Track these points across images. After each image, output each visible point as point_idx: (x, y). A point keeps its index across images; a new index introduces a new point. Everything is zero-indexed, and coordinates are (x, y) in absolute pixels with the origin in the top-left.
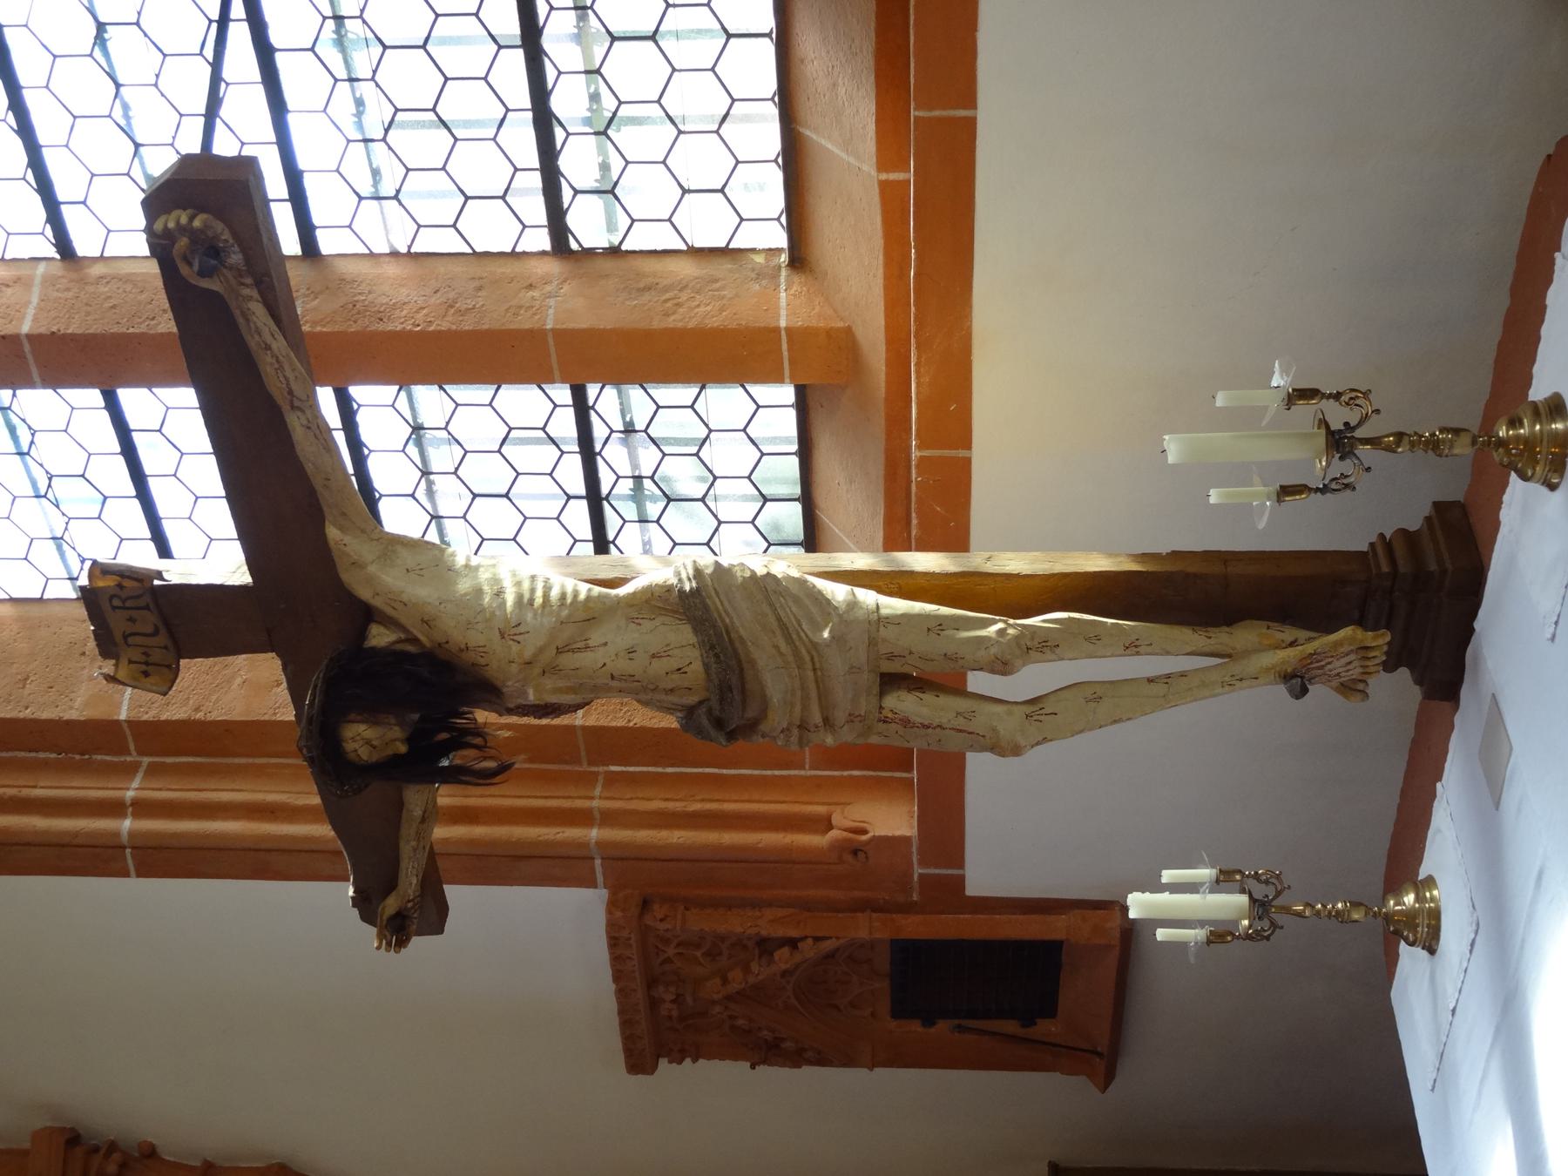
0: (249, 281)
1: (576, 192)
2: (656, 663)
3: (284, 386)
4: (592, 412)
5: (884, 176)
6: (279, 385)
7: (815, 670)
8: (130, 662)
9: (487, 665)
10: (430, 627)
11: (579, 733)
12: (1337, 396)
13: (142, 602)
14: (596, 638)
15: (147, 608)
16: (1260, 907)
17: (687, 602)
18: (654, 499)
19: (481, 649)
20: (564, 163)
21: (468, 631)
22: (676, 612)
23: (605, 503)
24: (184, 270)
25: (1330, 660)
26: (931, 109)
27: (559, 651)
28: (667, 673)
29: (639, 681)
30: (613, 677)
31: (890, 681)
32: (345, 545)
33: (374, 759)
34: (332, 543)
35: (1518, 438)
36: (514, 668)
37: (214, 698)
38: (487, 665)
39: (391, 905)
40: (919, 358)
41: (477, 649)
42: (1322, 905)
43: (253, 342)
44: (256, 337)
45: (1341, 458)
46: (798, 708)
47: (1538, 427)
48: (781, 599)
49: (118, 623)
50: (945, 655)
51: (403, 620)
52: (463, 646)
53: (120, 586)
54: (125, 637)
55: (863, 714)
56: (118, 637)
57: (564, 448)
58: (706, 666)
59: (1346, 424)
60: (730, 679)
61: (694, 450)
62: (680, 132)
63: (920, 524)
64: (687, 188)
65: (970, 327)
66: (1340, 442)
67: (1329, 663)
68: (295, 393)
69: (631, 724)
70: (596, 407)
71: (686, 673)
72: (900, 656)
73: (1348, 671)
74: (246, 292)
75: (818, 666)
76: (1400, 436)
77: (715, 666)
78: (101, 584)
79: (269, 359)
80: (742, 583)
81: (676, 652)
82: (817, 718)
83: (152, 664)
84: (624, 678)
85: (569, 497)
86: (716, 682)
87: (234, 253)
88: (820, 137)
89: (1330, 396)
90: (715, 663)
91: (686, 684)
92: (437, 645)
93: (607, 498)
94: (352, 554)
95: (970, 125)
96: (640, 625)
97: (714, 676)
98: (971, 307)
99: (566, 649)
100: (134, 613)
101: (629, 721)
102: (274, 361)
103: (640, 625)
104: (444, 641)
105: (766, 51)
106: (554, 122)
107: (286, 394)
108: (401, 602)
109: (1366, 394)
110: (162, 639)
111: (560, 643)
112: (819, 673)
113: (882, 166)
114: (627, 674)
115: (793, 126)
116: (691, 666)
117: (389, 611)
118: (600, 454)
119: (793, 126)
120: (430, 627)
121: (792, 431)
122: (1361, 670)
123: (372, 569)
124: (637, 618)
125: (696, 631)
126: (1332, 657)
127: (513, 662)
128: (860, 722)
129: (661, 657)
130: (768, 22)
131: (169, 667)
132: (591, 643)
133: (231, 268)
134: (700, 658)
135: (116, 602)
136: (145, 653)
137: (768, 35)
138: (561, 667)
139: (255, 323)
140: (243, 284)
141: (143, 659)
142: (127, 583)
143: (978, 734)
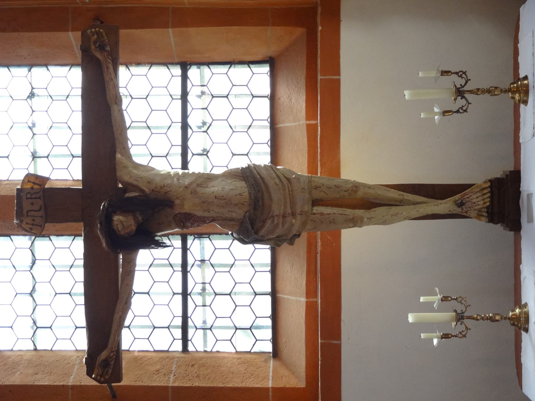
0: (110, 58)
1: (193, 155)
3: (115, 94)
5: (308, 122)
6: (113, 93)
7: (289, 191)
8: (27, 224)
11: (170, 390)
12: (457, 73)
13: (38, 195)
14: (211, 184)
15: (40, 198)
16: (460, 318)
18: (210, 294)
19: (169, 185)
20: (190, 143)
23: (189, 297)
24: (93, 47)
25: (471, 194)
26: (325, 76)
27: (197, 185)
30: (216, 197)
31: (316, 203)
33: (122, 233)
35: (514, 87)
36: (181, 189)
37: (7, 378)
38: (171, 191)
39: (104, 355)
40: (321, 170)
42: (484, 315)
43: (107, 78)
44: (110, 76)
45: (461, 99)
46: (282, 208)
47: (519, 83)
48: (278, 171)
49: (26, 205)
50: (335, 185)
51: (140, 185)
52: (162, 186)
53: (32, 188)
54: (27, 212)
55: (306, 211)
56: (25, 212)
57: (175, 269)
58: (250, 194)
59: (461, 85)
60: (258, 196)
61: (228, 269)
62: (234, 132)
63: (322, 245)
64: (234, 153)
65: (340, 158)
66: (460, 92)
67: (471, 196)
68: (117, 98)
69: (194, 385)
70: (190, 249)
71: (242, 195)
72: (319, 187)
73: (478, 202)
74: (109, 61)
75: (290, 190)
76: (478, 89)
77: (253, 191)
78: (25, 187)
79: (112, 84)
80: (264, 166)
81: (239, 188)
82: (289, 211)
83: (34, 225)
85: (174, 294)
87: (108, 47)
88: (284, 124)
89: (454, 73)
90: (253, 190)
93: (190, 294)
95: (338, 81)
98: (339, 149)
99: (200, 185)
100: (34, 201)
101: (193, 385)
102: (113, 85)
103: (226, 181)
104: (155, 187)
105: (266, 103)
106: (189, 128)
107: (115, 97)
108: (140, 177)
109: (465, 73)
110: (42, 213)
111: (198, 182)
112: (291, 193)
113: (307, 119)
115: (274, 127)
117: (135, 183)
118: (189, 272)
119: (274, 127)
120: (150, 184)
121: (269, 261)
122: (482, 202)
123: (130, 169)
125: (246, 183)
126: (471, 193)
127: (181, 187)
128: (305, 214)
130: (267, 91)
131: (41, 226)
132: (209, 186)
133: (107, 51)
134: (248, 191)
135: (29, 196)
136: (33, 220)
137: (267, 97)
139: (110, 71)
140: (109, 58)
141: (31, 222)
142: (36, 187)
143: (348, 215)
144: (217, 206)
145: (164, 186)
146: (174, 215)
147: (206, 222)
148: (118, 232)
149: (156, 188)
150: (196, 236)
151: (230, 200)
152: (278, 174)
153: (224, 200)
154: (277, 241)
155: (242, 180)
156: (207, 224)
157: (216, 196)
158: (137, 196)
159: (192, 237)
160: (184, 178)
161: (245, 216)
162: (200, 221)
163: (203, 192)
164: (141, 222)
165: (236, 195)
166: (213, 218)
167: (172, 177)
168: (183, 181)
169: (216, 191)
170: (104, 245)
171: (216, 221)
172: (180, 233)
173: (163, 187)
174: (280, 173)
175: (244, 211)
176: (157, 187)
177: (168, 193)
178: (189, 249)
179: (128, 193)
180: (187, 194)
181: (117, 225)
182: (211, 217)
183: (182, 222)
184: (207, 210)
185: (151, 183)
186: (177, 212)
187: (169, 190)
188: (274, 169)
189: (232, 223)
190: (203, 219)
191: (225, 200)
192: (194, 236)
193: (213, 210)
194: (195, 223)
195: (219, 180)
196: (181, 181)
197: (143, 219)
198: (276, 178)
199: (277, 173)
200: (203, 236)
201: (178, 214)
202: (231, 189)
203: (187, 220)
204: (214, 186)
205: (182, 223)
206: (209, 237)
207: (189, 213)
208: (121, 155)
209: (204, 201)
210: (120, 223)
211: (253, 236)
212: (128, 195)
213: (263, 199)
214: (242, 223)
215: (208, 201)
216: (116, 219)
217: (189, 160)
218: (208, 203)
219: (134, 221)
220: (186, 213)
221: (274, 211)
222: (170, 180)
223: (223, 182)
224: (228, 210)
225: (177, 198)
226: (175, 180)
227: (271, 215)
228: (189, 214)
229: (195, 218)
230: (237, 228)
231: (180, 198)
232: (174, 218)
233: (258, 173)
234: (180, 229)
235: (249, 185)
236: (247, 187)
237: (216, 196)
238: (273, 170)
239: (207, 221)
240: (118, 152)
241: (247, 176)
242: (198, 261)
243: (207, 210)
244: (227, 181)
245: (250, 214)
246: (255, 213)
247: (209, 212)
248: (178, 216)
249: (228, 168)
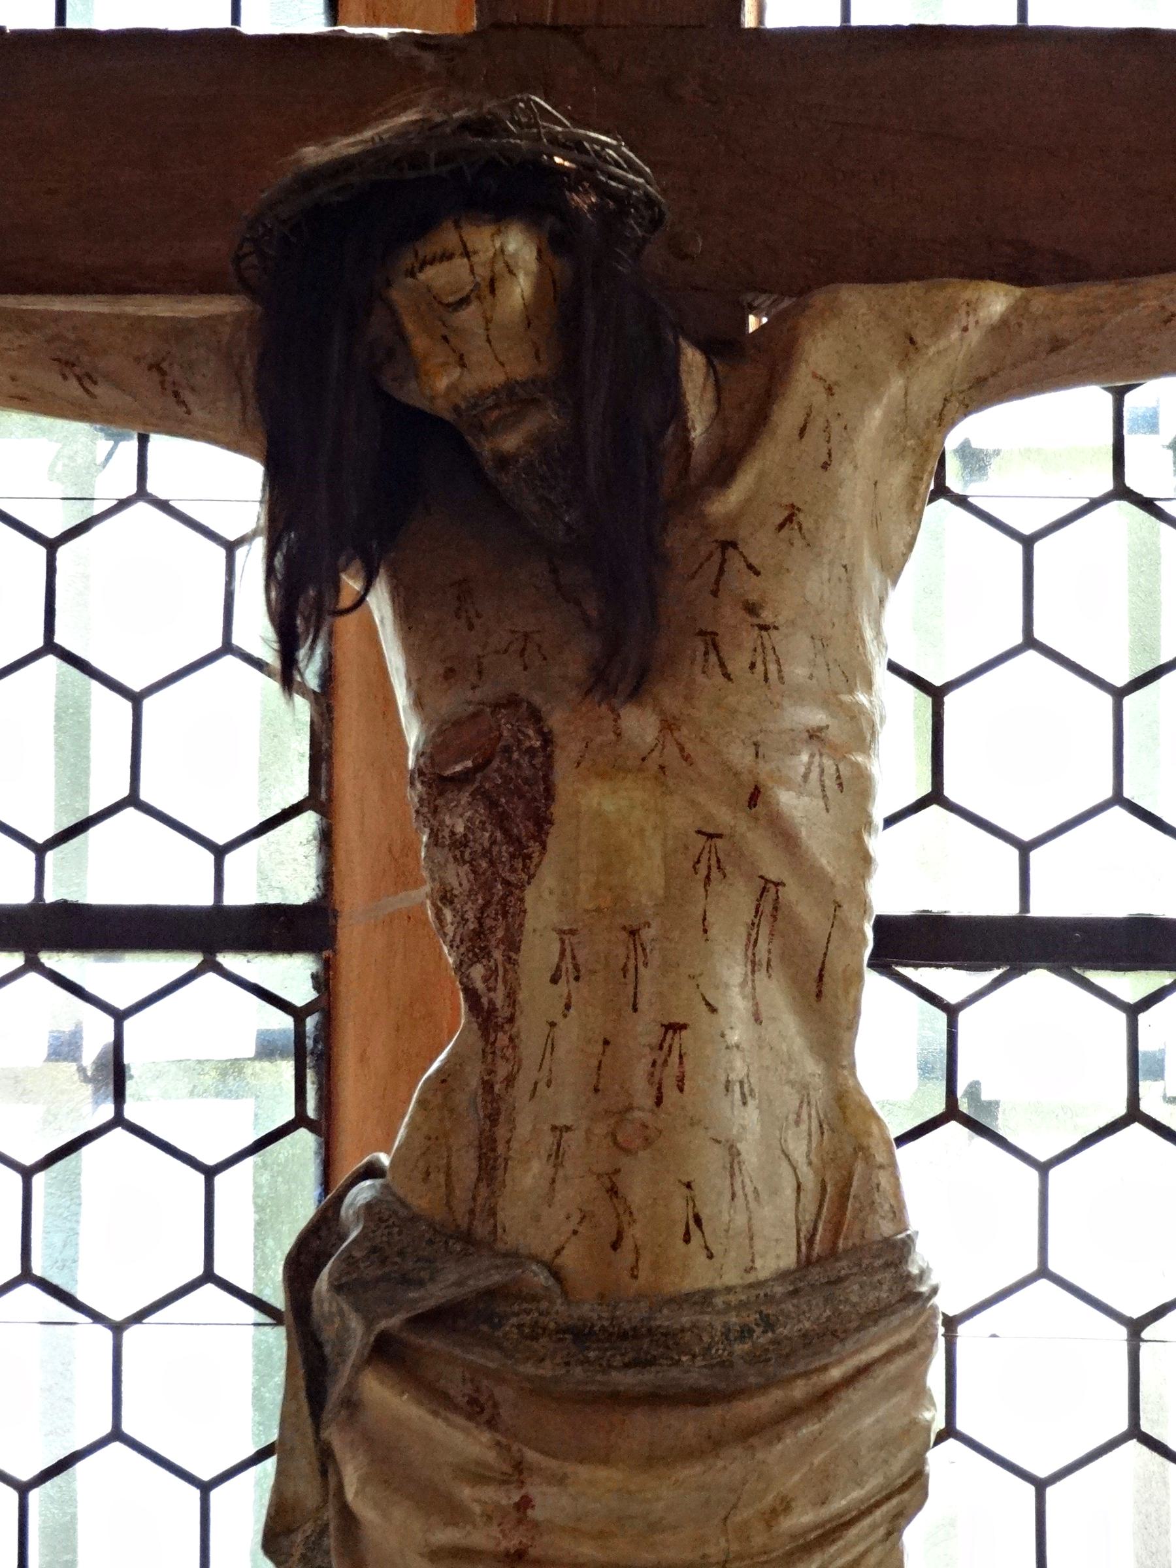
2: (715, 1157)
4: (192, 961)
9: (727, 676)
10: (781, 526)
17: (878, 1263)
19: (772, 667)
21: (808, 641)
22: (836, 1228)
27: (768, 887)
28: (688, 1186)
29: (659, 1101)
30: (676, 1028)
32: (965, 329)
34: (970, 291)
36: (740, 755)
38: (727, 676)
41: (771, 657)
48: (882, 1531)
52: (767, 616)
58: (705, 1298)
60: (678, 1363)
70: (211, 977)
71: (687, 1239)
77: (719, 1327)
80: (914, 1422)
81: (741, 1220)
84: (674, 1058)
86: (664, 1319)
91: (635, 1233)
92: (721, 535)
94: (942, 344)
96: (797, 1123)
97: (686, 1320)
99: (767, 908)
103: (797, 1123)
108: (830, 455)
111: (791, 893)
114: (688, 1067)
116: (702, 1257)
117: (787, 416)
118: (33, 964)
120: (781, 526)
123: (896, 385)
124: (810, 1116)
125: (783, 1276)
129: (732, 1176)
132: (761, 975)
134: (718, 1284)
138: (716, 886)
144: (606, 1042)
145: (764, 628)
146: (537, 699)
147: (477, 959)
148: (408, 260)
149: (750, 567)
150: (311, 1023)
151: (648, 1142)
152: (853, 1532)
153: (654, 1092)
154: (309, 1528)
155: (811, 1241)
156: (459, 966)
157: (684, 1027)
158: (686, 430)
159: (302, 993)
160: (830, 783)
161: (515, 1257)
162: (483, 909)
163: (713, 932)
164: (485, 448)
165: (688, 1186)
166: (507, 1013)
167: (836, 693)
168: (802, 770)
169: (723, 1036)
170: (312, 154)
171: (480, 1044)
172: (337, 896)
173: (756, 621)
174: (860, 1548)
175: (558, 1252)
176: (757, 573)
177: (713, 658)
178: (210, 965)
179: (710, 364)
180: (702, 798)
181: (467, 254)
182: (511, 997)
183: (478, 768)
184: (568, 964)
185: (784, 532)
186: (556, 720)
187: (738, 663)
188: (894, 1502)
189: (466, 1165)
190: (500, 933)
191: (649, 1102)
192: (309, 1009)
193: (568, 1006)
194: (467, 867)
195: (811, 1067)
196: (805, 758)
197: (503, 461)
198: (825, 1512)
199: (866, 1522)
200: (310, 1076)
201: (540, 732)
202: (733, 1153)
203: (492, 804)
204: (757, 1019)
205: (469, 764)
206: (300, 1120)
207: (551, 823)
208: (1004, 322)
209: (647, 934)
210: (482, 272)
211: (356, 1324)
212: (692, 359)
213: (656, 1399)
214: (467, 1238)
215: (646, 964)
216: (511, 247)
217: (908, 972)
218: (625, 970)
219: (495, 392)
220: (549, 794)
221: (561, 1480)
222: (811, 677)
223: (792, 1099)
224: (568, 1129)
225: (669, 725)
226: (817, 717)
227: (531, 1456)
228: (541, 823)
229: (513, 870)
230: (422, 1200)
231: (672, 750)
232: (512, 702)
233: (864, 1370)
234: (420, 755)
235: (770, 1299)
236: (751, 1278)
237: (684, 1033)
238: (888, 1498)
239: (477, 972)
240: (1026, 300)
241: (840, 1280)
242: (110, 1038)
243: (574, 958)
244: (804, 1127)
245: (535, 1298)
246: (544, 1341)
247: (555, 980)
248: (531, 732)
249: (902, 1140)
